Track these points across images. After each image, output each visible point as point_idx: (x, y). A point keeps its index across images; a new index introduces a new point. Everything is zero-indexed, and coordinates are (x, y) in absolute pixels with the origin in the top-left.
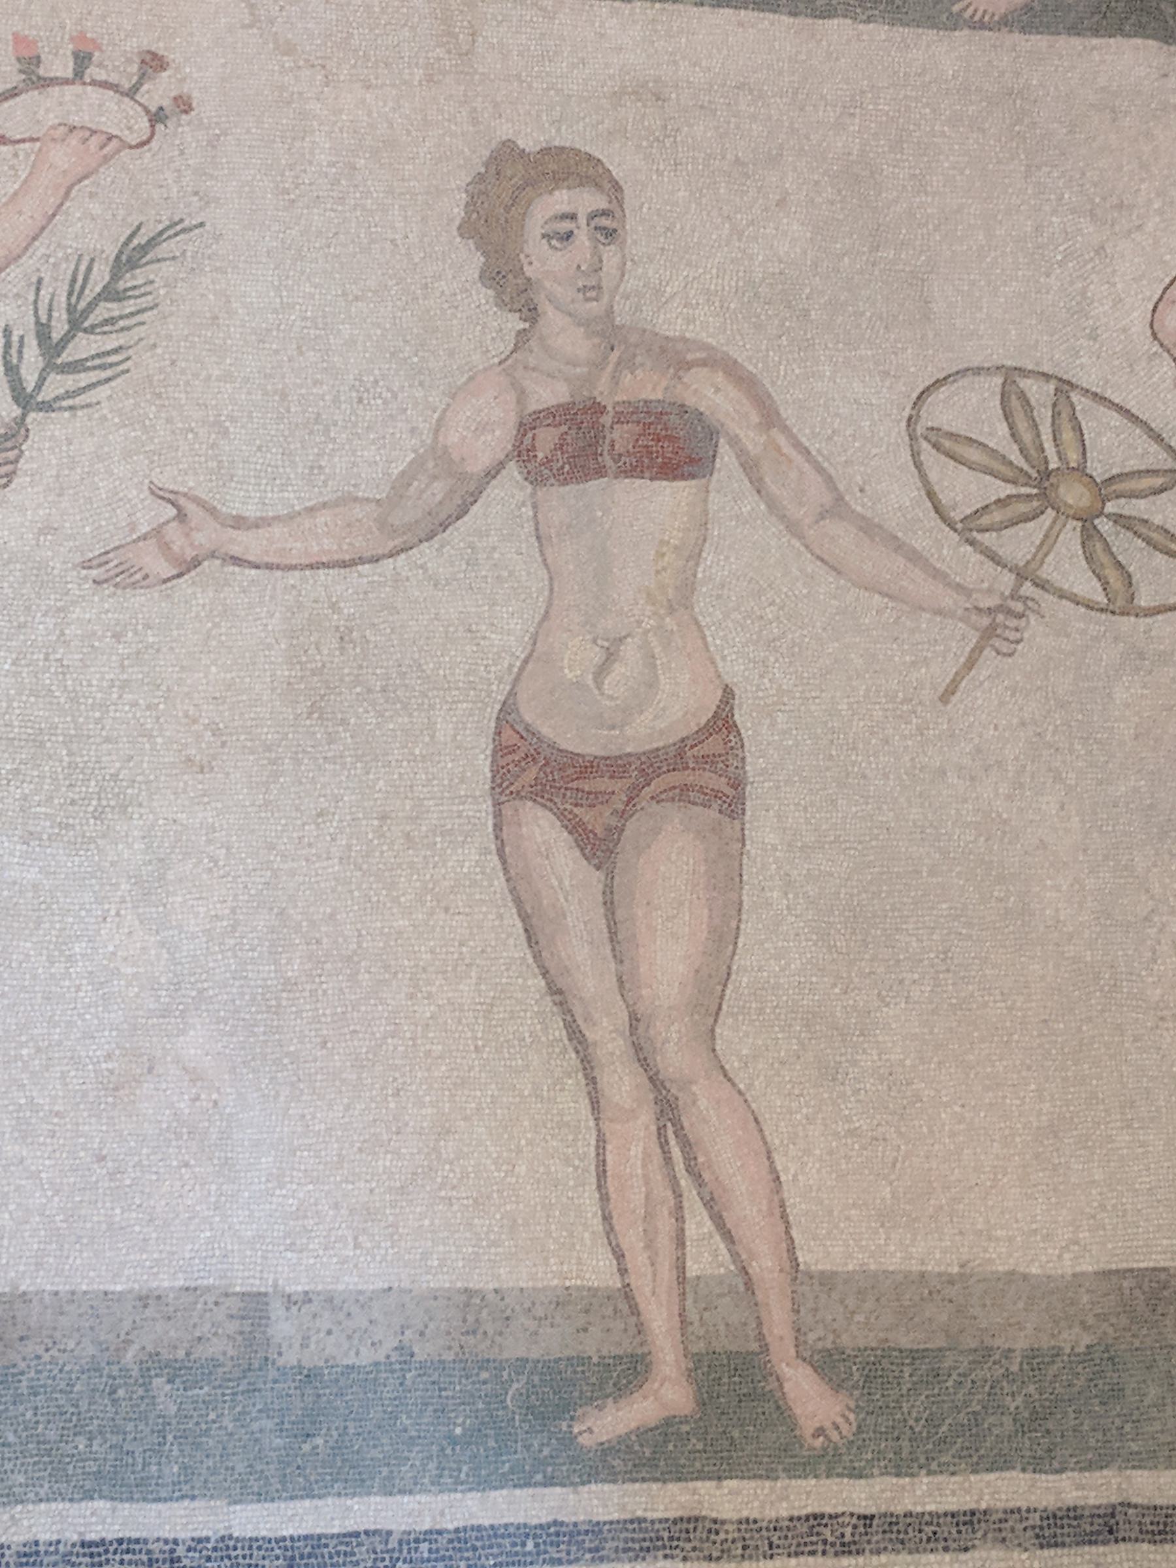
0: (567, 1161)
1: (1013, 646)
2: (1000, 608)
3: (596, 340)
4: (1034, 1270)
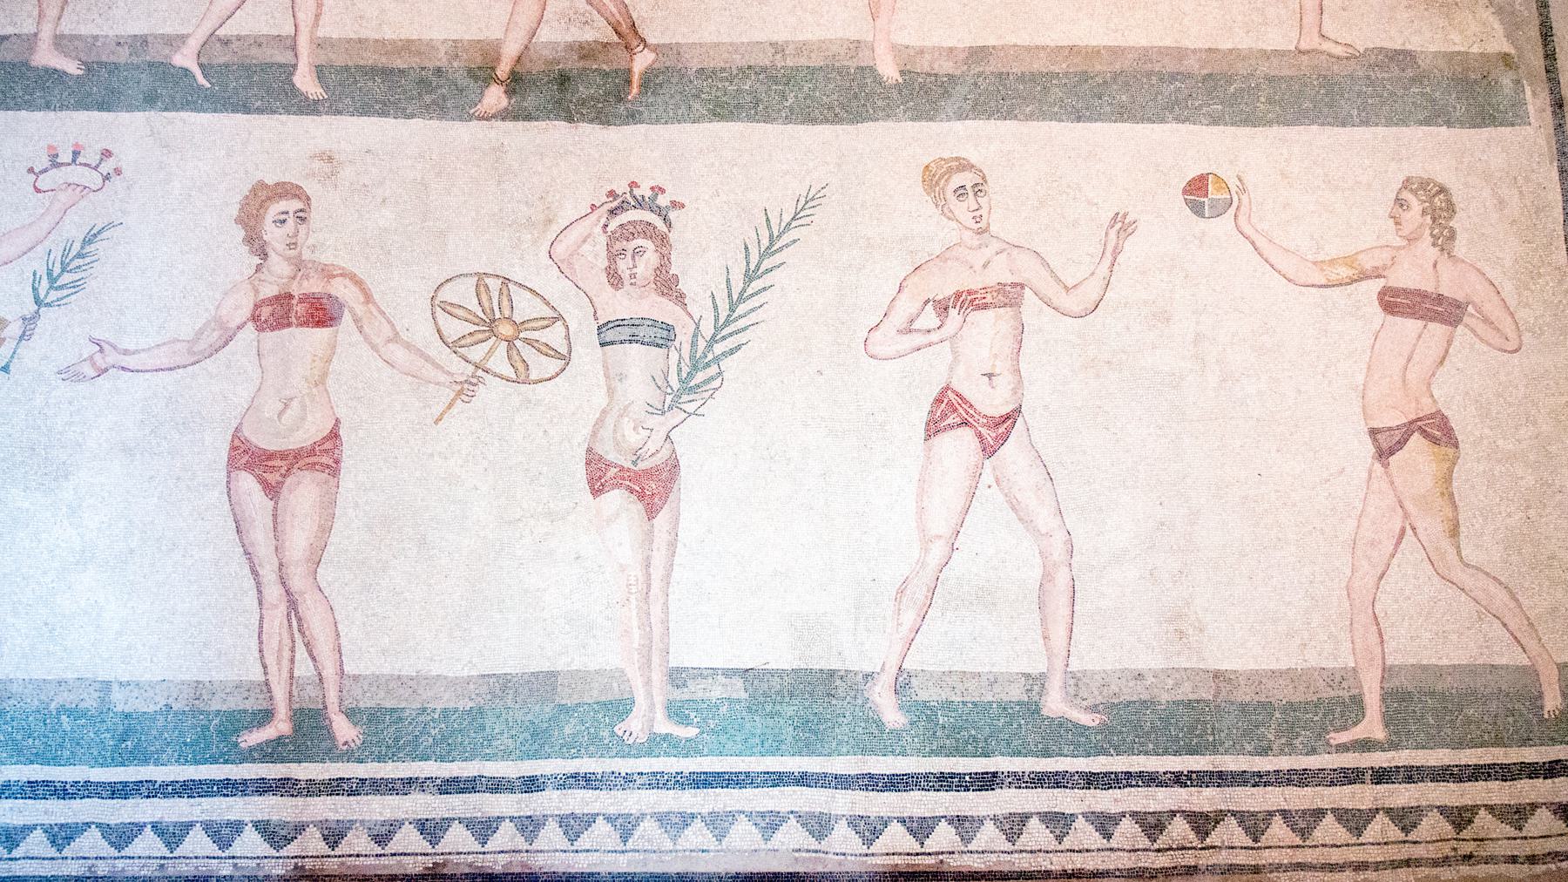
0: (246, 626)
1: (470, 398)
3: (292, 267)
4: (450, 675)
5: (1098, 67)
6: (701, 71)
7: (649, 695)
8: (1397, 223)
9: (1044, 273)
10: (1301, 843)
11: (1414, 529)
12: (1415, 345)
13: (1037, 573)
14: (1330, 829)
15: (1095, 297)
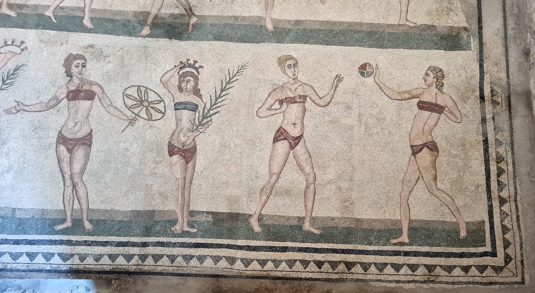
0: (59, 192)
2: (132, 119)
4: (122, 210)
5: (335, 28)
6: (211, 24)
7: (183, 218)
8: (425, 81)
9: (313, 92)
10: (380, 273)
11: (422, 177)
12: (428, 120)
13: (305, 186)
14: (389, 270)
15: (329, 100)
